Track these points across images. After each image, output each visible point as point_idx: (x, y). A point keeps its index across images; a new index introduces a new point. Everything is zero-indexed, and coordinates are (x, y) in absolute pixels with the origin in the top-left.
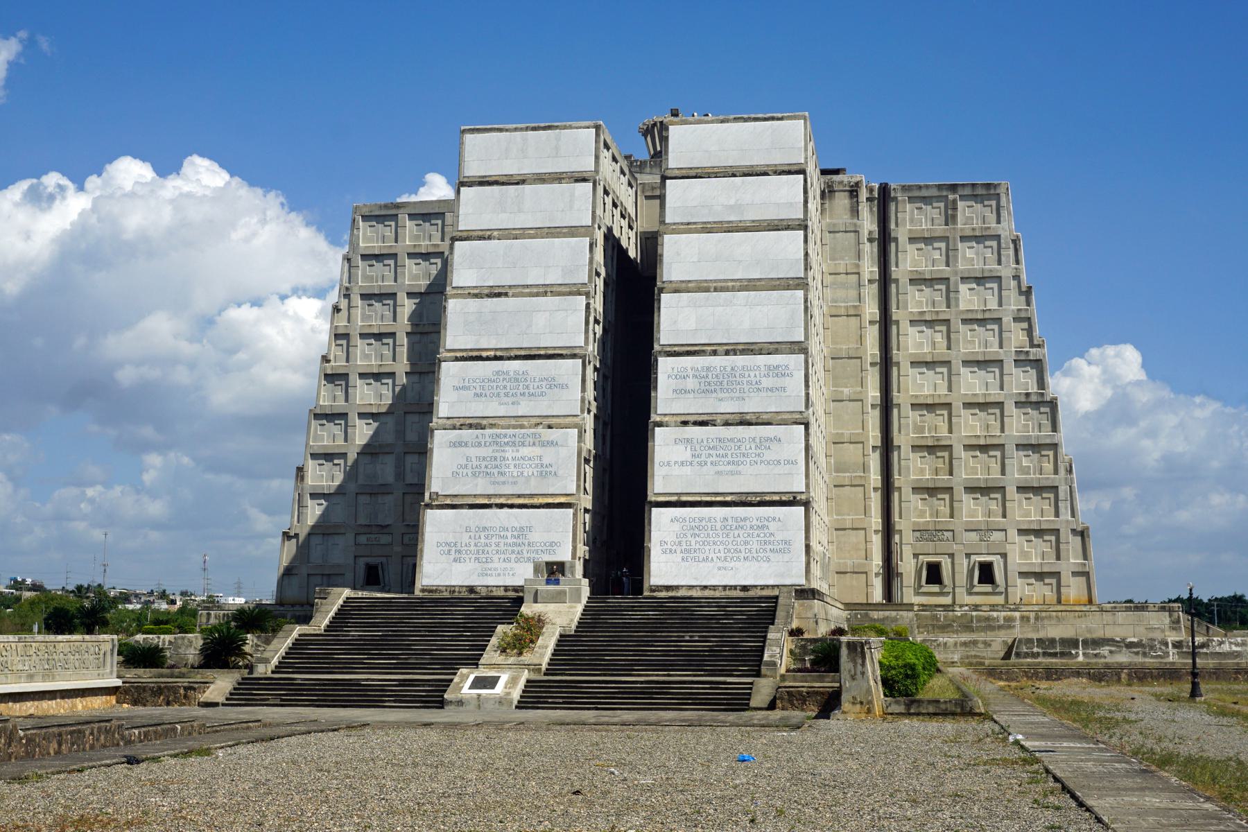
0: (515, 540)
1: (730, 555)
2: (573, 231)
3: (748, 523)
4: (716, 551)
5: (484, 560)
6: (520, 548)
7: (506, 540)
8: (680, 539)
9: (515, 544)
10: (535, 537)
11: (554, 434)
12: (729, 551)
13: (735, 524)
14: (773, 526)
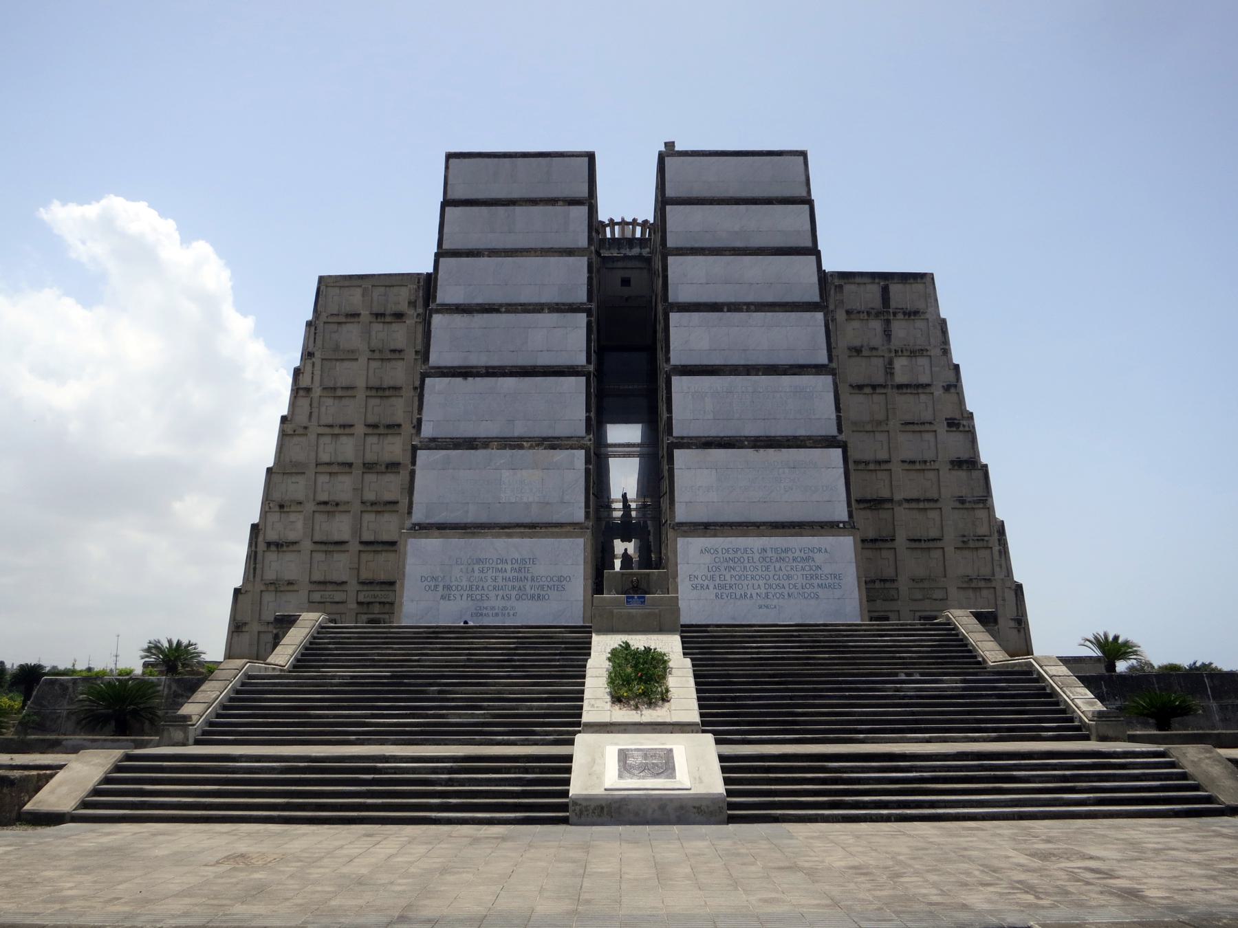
0: (516, 574)
1: (772, 591)
2: (569, 252)
3: (790, 555)
4: (756, 586)
5: (478, 597)
6: (521, 584)
7: (505, 575)
8: (712, 573)
9: (517, 579)
10: (540, 570)
11: (560, 455)
12: (771, 586)
13: (776, 555)
14: (819, 558)
